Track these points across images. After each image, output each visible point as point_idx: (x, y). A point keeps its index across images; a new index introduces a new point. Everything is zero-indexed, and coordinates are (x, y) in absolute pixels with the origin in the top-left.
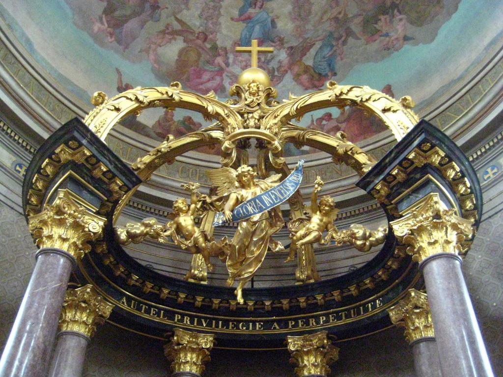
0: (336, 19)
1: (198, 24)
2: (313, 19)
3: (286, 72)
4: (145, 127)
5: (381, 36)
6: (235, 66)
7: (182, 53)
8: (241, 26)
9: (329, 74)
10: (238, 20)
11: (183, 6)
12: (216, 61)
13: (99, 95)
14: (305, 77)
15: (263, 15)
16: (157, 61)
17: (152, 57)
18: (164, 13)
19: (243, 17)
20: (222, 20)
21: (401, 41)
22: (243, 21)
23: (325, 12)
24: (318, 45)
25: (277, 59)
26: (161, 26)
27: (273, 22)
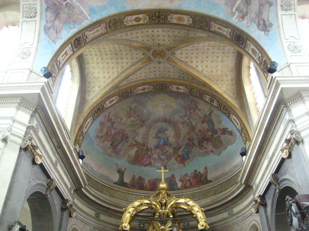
0: (189, 139)
1: (141, 141)
2: (181, 138)
3: (172, 156)
4: (127, 183)
5: (204, 148)
6: (155, 155)
7: (137, 152)
8: (157, 140)
9: (187, 158)
10: (155, 138)
11: (136, 136)
12: (148, 153)
13: (125, 209)
14: (179, 159)
15: (164, 136)
16: (129, 157)
17: (127, 156)
18: (130, 139)
19: (157, 137)
20: (150, 138)
21: (210, 152)
22: (157, 138)
23: (185, 136)
24: (183, 147)
25: (169, 152)
26: (129, 144)
27: (167, 138)
